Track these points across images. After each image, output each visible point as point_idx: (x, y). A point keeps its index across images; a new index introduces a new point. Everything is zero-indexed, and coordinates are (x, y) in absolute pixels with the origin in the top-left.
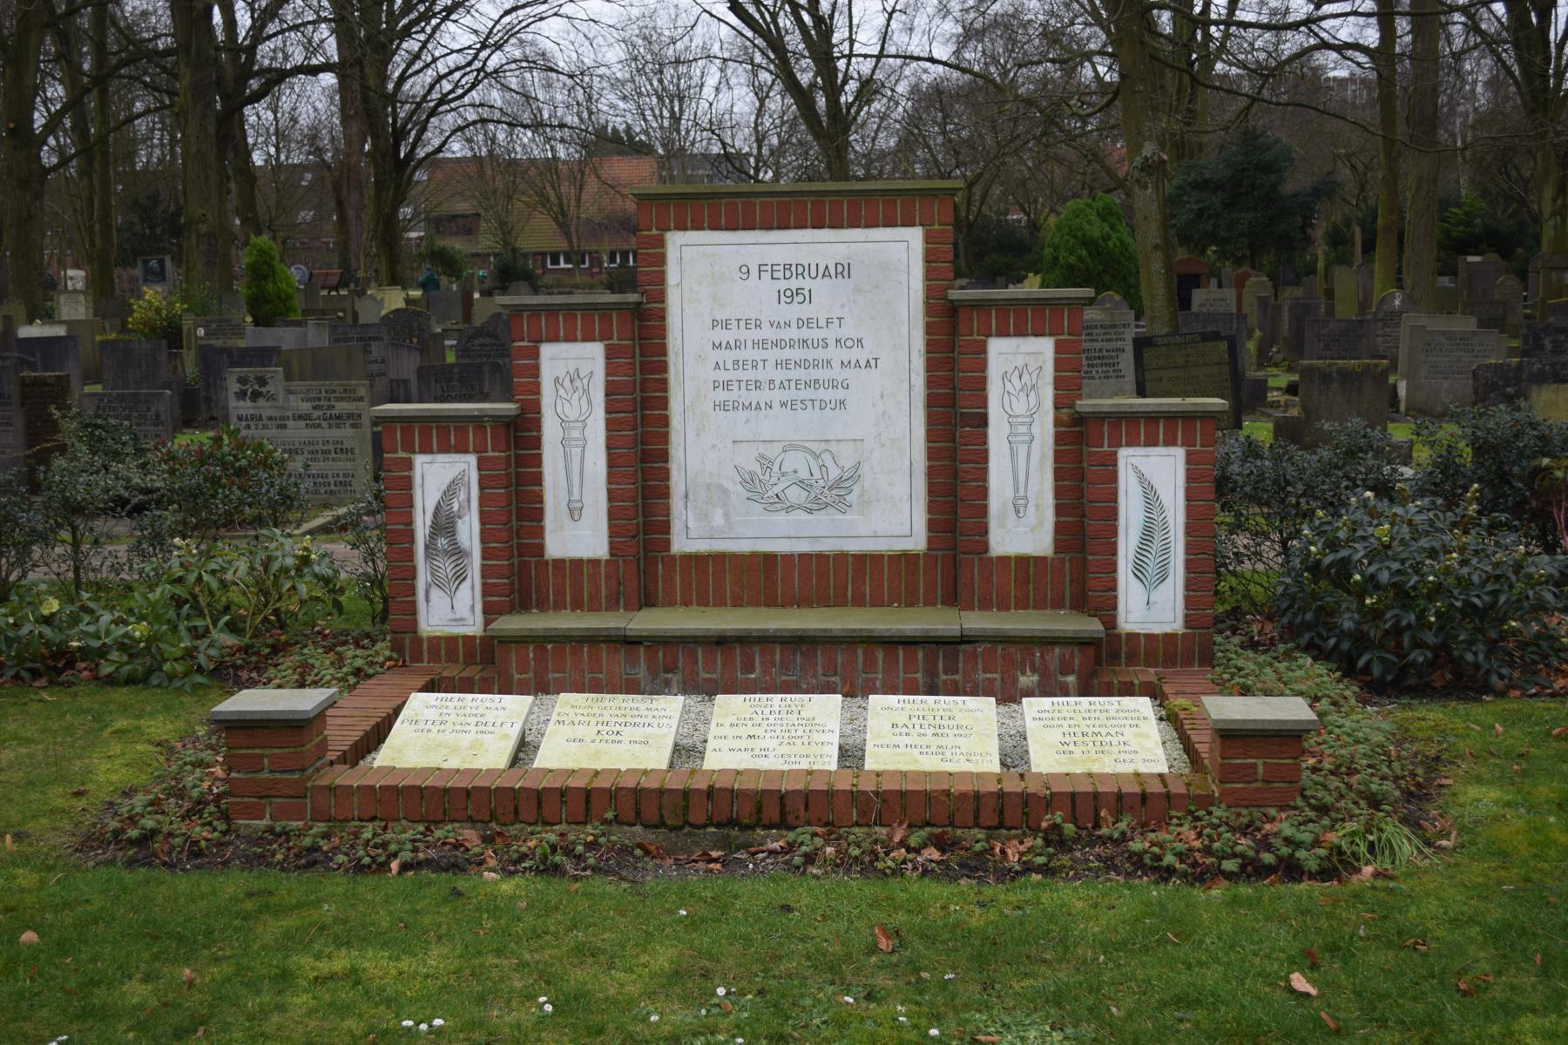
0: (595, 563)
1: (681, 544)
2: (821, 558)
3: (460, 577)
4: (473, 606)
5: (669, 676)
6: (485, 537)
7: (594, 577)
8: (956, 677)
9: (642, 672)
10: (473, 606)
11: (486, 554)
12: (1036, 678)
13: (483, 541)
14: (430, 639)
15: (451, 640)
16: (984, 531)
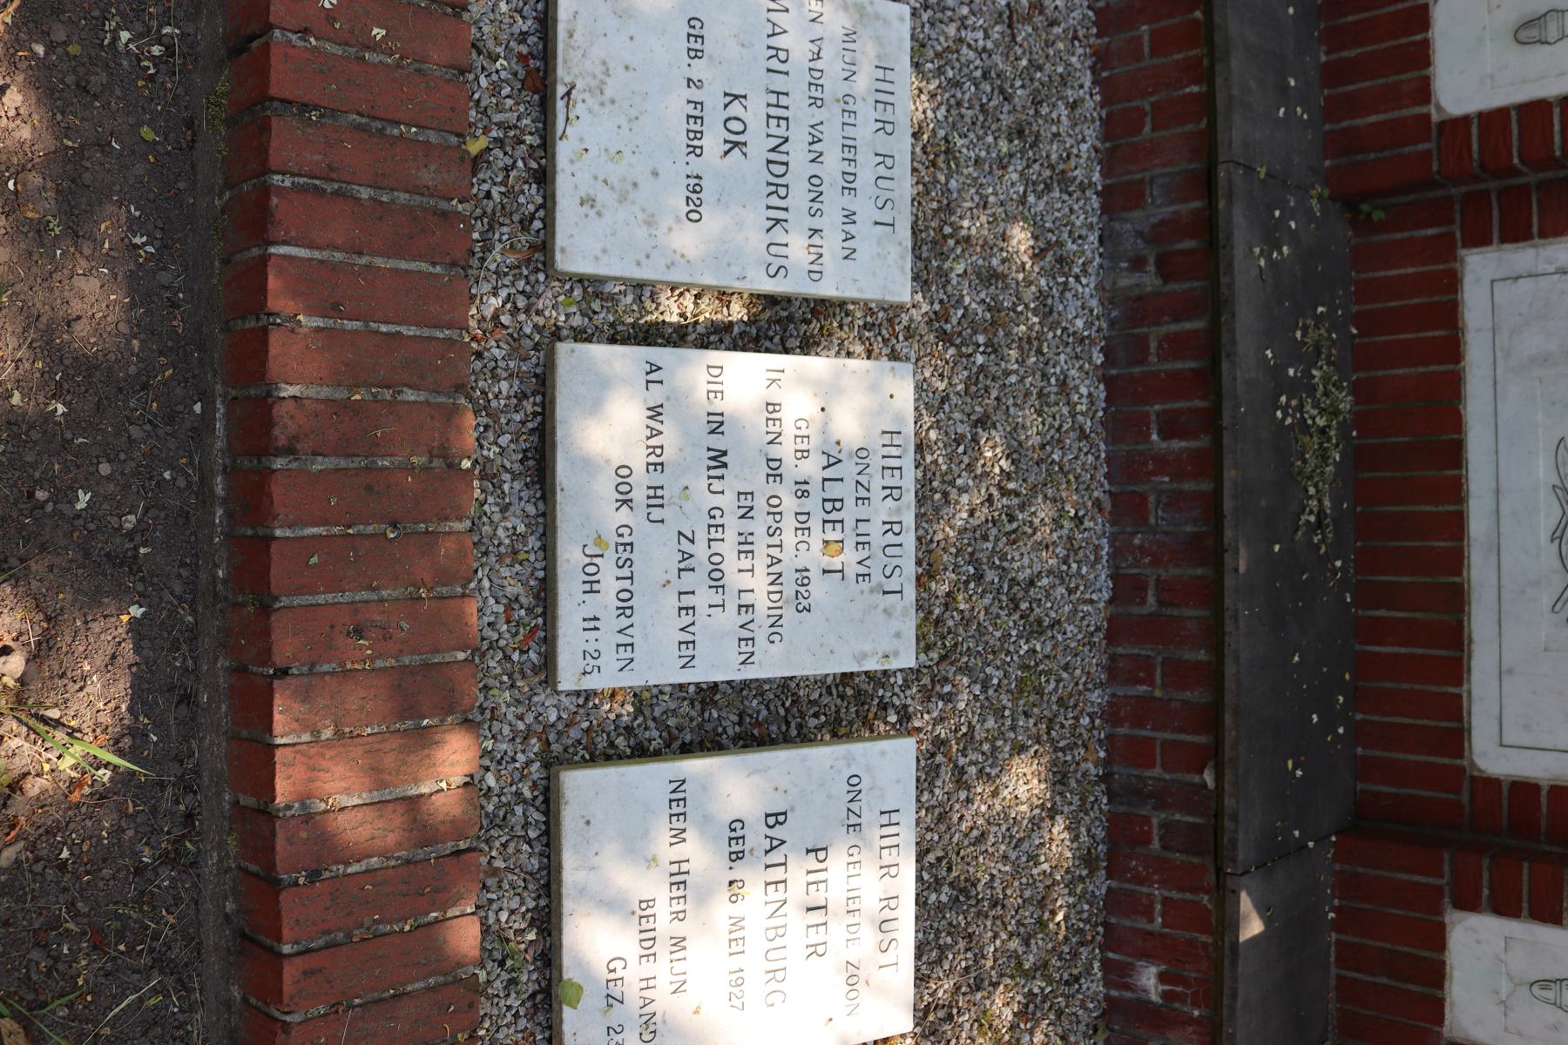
0: (1424, 92)
2: (1456, 560)
5: (1151, 268)
8: (1156, 845)
9: (1158, 208)
12: (1154, 997)
16: (1505, 907)
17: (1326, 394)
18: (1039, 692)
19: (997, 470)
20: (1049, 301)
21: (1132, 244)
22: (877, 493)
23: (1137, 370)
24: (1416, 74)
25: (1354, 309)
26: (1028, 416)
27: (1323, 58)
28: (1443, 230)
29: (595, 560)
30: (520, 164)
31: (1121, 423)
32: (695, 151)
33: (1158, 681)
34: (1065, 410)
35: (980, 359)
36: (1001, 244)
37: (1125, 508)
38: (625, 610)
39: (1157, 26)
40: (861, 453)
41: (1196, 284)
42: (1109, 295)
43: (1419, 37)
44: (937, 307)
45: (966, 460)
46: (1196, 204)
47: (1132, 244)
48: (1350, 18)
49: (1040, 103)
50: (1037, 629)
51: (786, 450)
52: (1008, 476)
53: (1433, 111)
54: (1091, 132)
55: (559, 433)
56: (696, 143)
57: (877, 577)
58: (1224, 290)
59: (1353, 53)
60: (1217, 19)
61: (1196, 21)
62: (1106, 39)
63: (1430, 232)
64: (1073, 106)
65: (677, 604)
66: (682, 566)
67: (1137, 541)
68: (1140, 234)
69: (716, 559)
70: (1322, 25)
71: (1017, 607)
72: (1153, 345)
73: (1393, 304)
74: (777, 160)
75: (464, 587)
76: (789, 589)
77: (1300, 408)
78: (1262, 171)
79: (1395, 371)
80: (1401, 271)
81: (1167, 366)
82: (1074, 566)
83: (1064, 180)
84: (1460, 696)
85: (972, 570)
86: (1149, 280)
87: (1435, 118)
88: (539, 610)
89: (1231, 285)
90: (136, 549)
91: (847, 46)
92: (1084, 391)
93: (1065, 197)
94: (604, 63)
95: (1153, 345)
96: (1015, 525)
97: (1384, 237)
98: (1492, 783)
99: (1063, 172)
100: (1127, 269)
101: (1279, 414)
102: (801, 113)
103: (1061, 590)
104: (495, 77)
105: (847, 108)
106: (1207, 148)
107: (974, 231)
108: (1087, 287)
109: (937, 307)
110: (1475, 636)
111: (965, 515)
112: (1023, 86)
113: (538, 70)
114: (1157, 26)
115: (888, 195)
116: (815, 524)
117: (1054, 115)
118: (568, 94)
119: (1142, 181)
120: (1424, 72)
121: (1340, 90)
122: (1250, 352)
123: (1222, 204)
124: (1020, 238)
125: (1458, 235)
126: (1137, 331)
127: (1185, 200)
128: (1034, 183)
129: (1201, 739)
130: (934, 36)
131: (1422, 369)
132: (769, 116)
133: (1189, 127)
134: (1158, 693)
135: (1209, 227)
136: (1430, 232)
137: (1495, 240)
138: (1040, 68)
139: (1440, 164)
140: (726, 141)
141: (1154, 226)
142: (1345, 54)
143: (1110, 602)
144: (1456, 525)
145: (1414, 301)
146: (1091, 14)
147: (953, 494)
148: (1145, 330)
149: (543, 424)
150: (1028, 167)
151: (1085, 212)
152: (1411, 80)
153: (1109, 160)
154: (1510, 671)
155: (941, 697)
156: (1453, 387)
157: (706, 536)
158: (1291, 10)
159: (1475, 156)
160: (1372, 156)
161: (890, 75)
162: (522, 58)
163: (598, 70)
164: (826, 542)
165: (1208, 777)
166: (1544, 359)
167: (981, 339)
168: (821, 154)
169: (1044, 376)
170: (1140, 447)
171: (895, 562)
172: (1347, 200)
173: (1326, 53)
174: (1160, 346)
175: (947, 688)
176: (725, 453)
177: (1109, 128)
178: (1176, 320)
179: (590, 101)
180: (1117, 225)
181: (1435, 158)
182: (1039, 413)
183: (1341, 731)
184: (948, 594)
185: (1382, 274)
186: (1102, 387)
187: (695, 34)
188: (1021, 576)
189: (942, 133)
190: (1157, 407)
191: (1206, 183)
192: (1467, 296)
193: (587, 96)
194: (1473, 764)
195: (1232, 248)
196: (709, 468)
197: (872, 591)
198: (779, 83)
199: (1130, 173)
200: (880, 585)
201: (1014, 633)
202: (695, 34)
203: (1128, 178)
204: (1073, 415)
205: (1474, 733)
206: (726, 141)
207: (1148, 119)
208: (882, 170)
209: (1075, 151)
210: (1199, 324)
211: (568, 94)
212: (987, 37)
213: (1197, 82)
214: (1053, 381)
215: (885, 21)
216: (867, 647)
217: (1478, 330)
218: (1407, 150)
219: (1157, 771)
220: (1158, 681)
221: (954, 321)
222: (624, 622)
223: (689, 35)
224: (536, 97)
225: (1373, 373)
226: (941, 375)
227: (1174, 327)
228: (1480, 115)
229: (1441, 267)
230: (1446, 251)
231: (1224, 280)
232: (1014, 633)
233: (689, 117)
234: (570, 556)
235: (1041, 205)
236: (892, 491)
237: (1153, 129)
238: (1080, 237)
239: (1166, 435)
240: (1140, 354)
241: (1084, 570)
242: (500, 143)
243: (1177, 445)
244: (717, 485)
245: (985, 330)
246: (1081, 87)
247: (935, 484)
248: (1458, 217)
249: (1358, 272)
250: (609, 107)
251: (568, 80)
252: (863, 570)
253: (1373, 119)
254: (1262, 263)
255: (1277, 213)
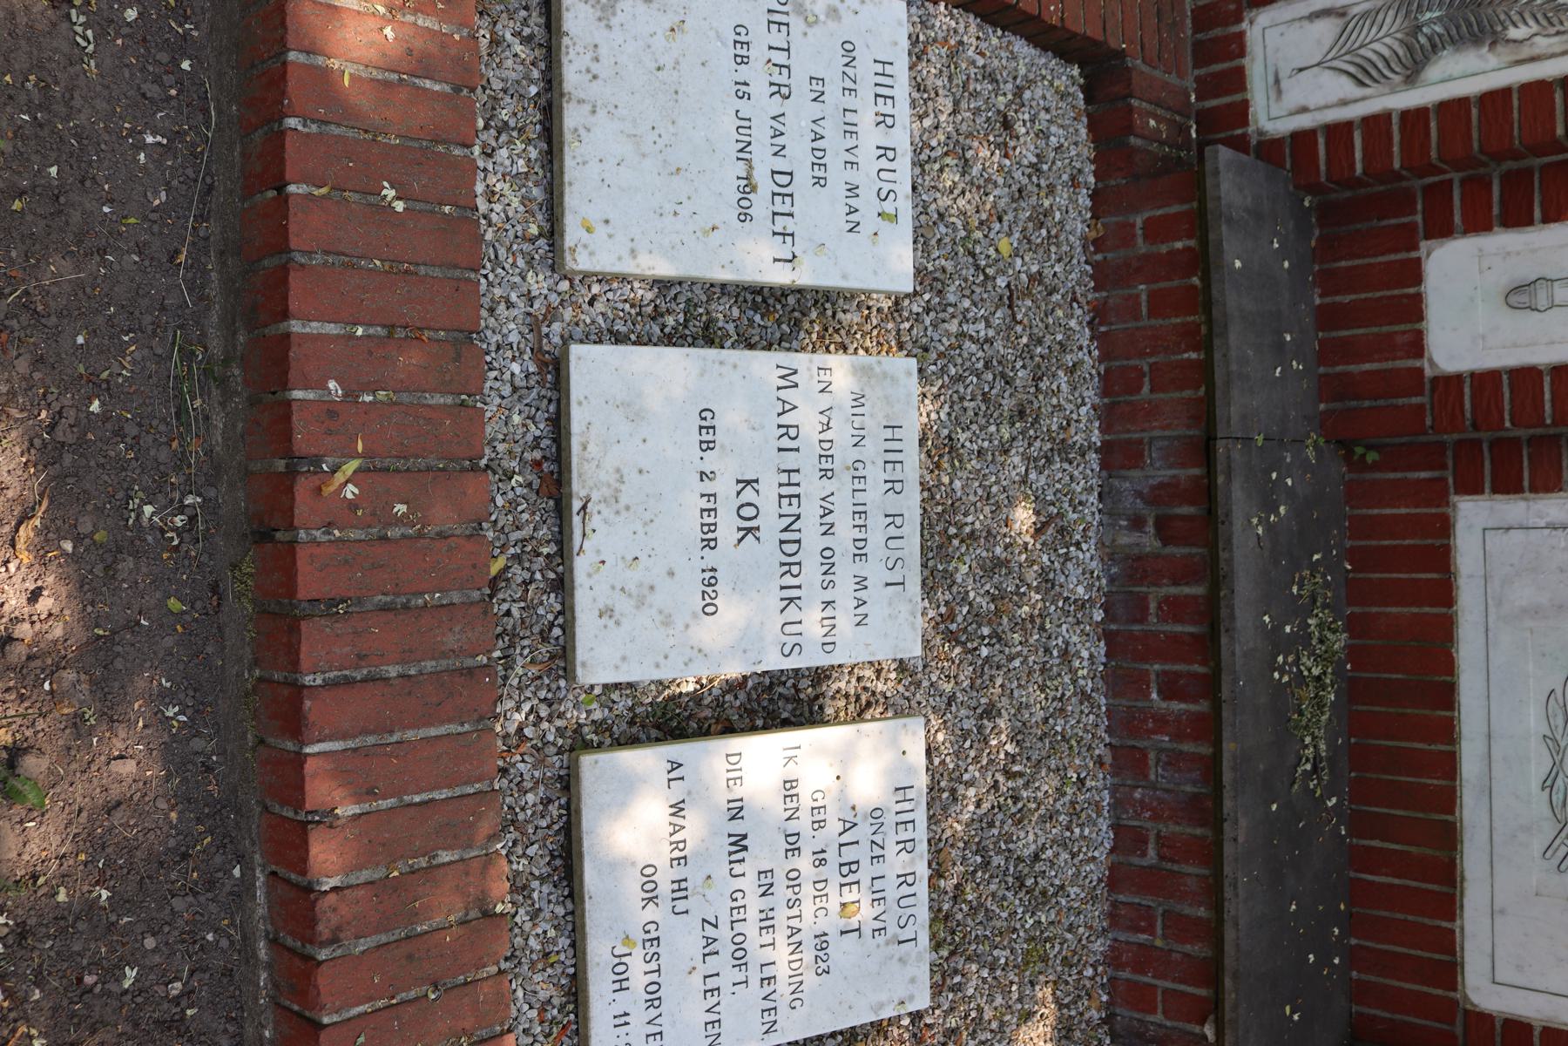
0: (1417, 346)
1: (1473, 517)
2: (1448, 799)
3: (1364, 75)
4: (1304, 110)
5: (1150, 528)
6: (1453, 109)
7: (1386, 347)
9: (1158, 471)
10: (1304, 110)
11: (1414, 119)
13: (1445, 107)
14: (1241, 36)
15: (1237, 79)
17: (1321, 641)
18: (1044, 959)
19: (1002, 756)
20: (1051, 576)
21: (1130, 503)
22: (891, 849)
23: (1136, 627)
24: (1408, 327)
25: (1348, 544)
26: (1034, 694)
27: (1318, 301)
28: (1436, 474)
29: (624, 960)
30: (538, 576)
31: (1121, 677)
32: (709, 544)
33: (1159, 931)
34: (1067, 679)
35: (985, 652)
36: (1005, 530)
37: (1126, 762)
38: (654, 1001)
39: (1155, 286)
40: (876, 813)
41: (1194, 550)
42: (1109, 553)
43: (1412, 290)
44: (943, 610)
45: (972, 753)
46: (1196, 471)
47: (1130, 503)
48: (1343, 264)
49: (1041, 379)
50: (1042, 899)
51: (803, 824)
52: (1012, 758)
53: (1426, 366)
54: (1090, 394)
55: (586, 844)
56: (710, 536)
57: (892, 929)
58: (1222, 564)
59: (1347, 298)
60: (1214, 292)
61: (1194, 287)
62: (1104, 294)
63: (1423, 475)
64: (1071, 370)
65: (703, 988)
66: (707, 951)
67: (1137, 795)
68: (1139, 494)
69: (739, 939)
70: (1317, 268)
71: (1022, 885)
72: (1153, 606)
73: (1386, 543)
74: (790, 540)
75: (502, 1024)
76: (808, 955)
77: (1297, 662)
78: (1260, 439)
79: (1389, 609)
80: (1395, 511)
81: (1167, 628)
82: (1077, 831)
83: (1063, 449)
84: (1453, 932)
85: (979, 859)
86: (1148, 541)
87: (1428, 372)
88: (571, 1007)
89: (1230, 561)
90: (183, 1011)
91: (856, 411)
92: (1085, 654)
93: (1066, 466)
94: (618, 470)
95: (1153, 606)
96: (1020, 805)
97: (1378, 475)
98: (1485, 1018)
99: (1063, 440)
100: (1126, 528)
101: (1276, 675)
102: (812, 487)
103: (1065, 856)
104: (511, 495)
105: (857, 474)
106: (1206, 414)
107: (977, 525)
108: (1088, 554)
109: (943, 610)
110: (1467, 874)
111: (971, 808)
112: (1024, 367)
113: (552, 473)
114: (1155, 286)
115: (899, 554)
116: (833, 889)
117: (1054, 387)
118: (584, 508)
119: (1140, 442)
120: (1417, 326)
121: (1334, 334)
122: (1248, 619)
123: (1221, 479)
124: (1023, 517)
125: (1451, 481)
126: (1137, 589)
127: (1183, 465)
128: (1035, 460)
129: (1202, 992)
130: (936, 337)
131: (1415, 610)
132: (781, 496)
133: (1187, 393)
134: (1159, 943)
135: (1207, 494)
136: (1423, 475)
137: (1487, 490)
138: (1040, 342)
139: (1434, 420)
140: (739, 529)
141: (1153, 488)
142: (1338, 298)
143: (1112, 851)
144: (1449, 765)
145: (1407, 542)
146: (1088, 268)
147: (961, 789)
148: (1144, 589)
149: (568, 822)
150: (1030, 445)
151: (1085, 476)
152: (1404, 333)
153: (1108, 416)
154: (1502, 912)
155: (951, 989)
156: (1445, 630)
157: (729, 919)
158: (1286, 264)
159: (1468, 415)
160: (1367, 403)
161: (898, 433)
162: (537, 464)
163: (612, 478)
164: (844, 905)
165: (1209, 1031)
166: (1535, 611)
167: (986, 631)
168: (832, 525)
169: (1047, 651)
170: (1139, 704)
171: (909, 911)
172: (1343, 438)
173: (1321, 296)
174: (1159, 607)
175: (957, 979)
176: (745, 837)
177: (1108, 384)
178: (1176, 583)
179: (606, 512)
180: (1116, 483)
181: (1428, 413)
182: (1042, 689)
183: (1336, 961)
184: (957, 887)
185: (1376, 511)
186: (1102, 644)
187: (707, 424)
188: (1026, 852)
189: (946, 432)
190: (1156, 667)
191: (1205, 450)
192: (1459, 542)
193: (602, 507)
194: (1466, 997)
195: (1231, 524)
196: (730, 854)
197: (887, 943)
198: (790, 460)
199: (1128, 431)
200: (895, 936)
201: (1020, 911)
202: (707, 424)
203: (1127, 436)
204: (1074, 682)
205: (1467, 968)
206: (739, 529)
207: (1147, 379)
208: (892, 531)
209: (1075, 416)
210: (1197, 590)
211: (584, 508)
212: (988, 325)
213: (1196, 349)
214: (1055, 653)
215: (892, 378)
216: (883, 997)
217: (1471, 576)
218: (1401, 401)
219: (1159, 1017)
220: (1159, 931)
221: (960, 619)
222: (653, 1013)
223: (701, 428)
224: (551, 503)
225: (1367, 609)
226: (948, 676)
227: (1173, 590)
228: (1473, 375)
229: (1433, 511)
230: (1438, 495)
231: (1223, 555)
232: (1020, 911)
233: (703, 510)
234: (599, 950)
235: (1043, 480)
236: (906, 845)
237: (1152, 391)
238: (1080, 503)
239: (1166, 694)
240: (1140, 614)
241: (1087, 832)
242: (517, 558)
243: (1177, 706)
244: (738, 869)
245: (990, 623)
246: (1080, 348)
247: (943, 784)
248: (1450, 463)
249: (1352, 507)
250: (624, 513)
251: (583, 493)
252: (878, 925)
253: (1367, 366)
254: (1260, 531)
255: (1274, 475)
